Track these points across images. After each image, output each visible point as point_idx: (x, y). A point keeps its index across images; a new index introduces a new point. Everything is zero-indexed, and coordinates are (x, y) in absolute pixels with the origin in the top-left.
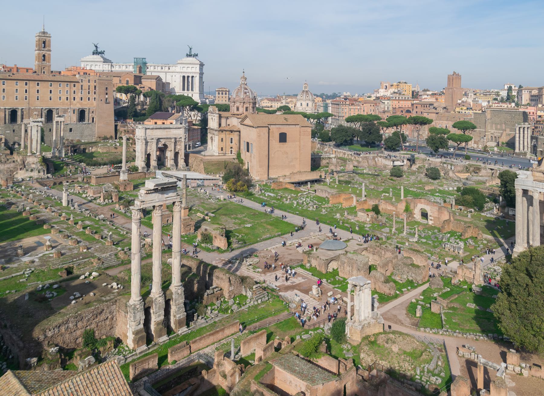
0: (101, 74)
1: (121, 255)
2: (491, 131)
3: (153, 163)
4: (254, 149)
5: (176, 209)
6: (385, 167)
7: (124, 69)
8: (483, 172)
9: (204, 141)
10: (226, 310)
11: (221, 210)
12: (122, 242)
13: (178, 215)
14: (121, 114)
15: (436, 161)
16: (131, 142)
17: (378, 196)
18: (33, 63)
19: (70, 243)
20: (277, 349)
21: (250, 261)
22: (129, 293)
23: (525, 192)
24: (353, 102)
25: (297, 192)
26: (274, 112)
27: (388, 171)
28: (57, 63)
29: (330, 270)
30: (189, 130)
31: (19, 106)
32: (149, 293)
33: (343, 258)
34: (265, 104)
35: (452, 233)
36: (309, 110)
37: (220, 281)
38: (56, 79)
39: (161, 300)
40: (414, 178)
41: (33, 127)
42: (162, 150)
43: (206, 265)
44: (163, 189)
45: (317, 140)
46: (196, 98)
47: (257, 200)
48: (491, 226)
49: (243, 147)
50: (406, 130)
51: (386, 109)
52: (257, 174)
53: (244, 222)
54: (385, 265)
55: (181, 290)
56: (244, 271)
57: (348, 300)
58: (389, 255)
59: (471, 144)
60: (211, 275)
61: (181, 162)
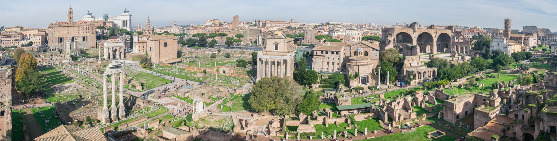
0: (90, 22)
1: (99, 92)
2: (249, 37)
3: (111, 57)
4: (153, 50)
5: (121, 75)
6: (208, 54)
7: (99, 19)
8: (246, 53)
9: (132, 47)
10: (142, 113)
11: (139, 75)
12: (100, 87)
13: (122, 77)
14: (98, 38)
15: (229, 51)
16: (102, 48)
17: (206, 66)
18: (67, 20)
19: (80, 86)
20: (164, 125)
21: (151, 95)
22: (103, 106)
23: (260, 59)
24: (195, 28)
25: (171, 67)
26: (162, 34)
27: (210, 56)
28: (75, 20)
29: (186, 96)
30: (126, 43)
31: (63, 36)
32: (110, 106)
33: (191, 92)
34: (158, 31)
35: (235, 77)
36: (177, 33)
37: (139, 102)
38: (75, 25)
39: (116, 109)
40: (220, 58)
41: (67, 43)
42: (115, 51)
43: (133, 97)
44: (116, 67)
45: (180, 45)
46: (128, 29)
47: (154, 71)
48: (249, 73)
49: (148, 49)
50: (217, 39)
51: (209, 31)
52: (154, 60)
53: (149, 80)
54: (209, 92)
55: (123, 105)
56: (150, 98)
57: (193, 107)
58: (210, 88)
59: (242, 43)
60: (135, 100)
61: (122, 56)
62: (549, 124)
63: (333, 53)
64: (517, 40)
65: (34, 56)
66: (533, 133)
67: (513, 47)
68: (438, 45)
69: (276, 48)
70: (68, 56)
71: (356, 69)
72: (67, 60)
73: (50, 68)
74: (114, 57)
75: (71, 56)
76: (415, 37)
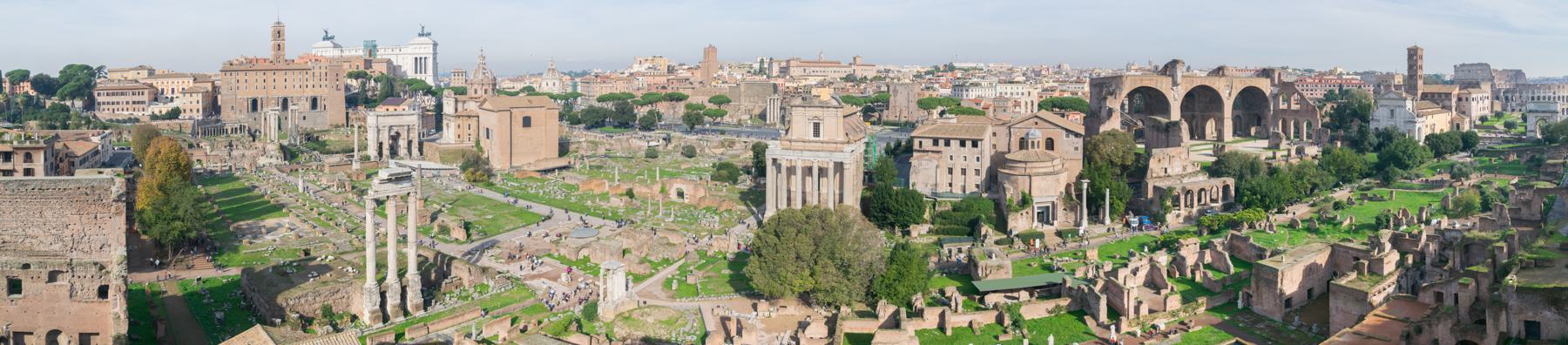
0: (331, 60)
1: (356, 242)
2: (745, 104)
3: (386, 152)
4: (494, 135)
5: (411, 199)
6: (640, 148)
7: (353, 53)
8: (738, 146)
9: (439, 128)
10: (466, 298)
11: (457, 202)
12: (356, 230)
13: (414, 205)
14: (352, 101)
15: (692, 139)
16: (363, 129)
17: (632, 180)
18: (269, 54)
19: (306, 227)
20: (523, 331)
21: (491, 252)
22: (365, 278)
23: (775, 160)
24: (605, 79)
25: (543, 181)
26: (516, 94)
27: (643, 153)
28: (290, 53)
29: (581, 257)
30: (423, 117)
31: (259, 95)
33: (595, 245)
34: (506, 85)
35: (708, 209)
36: (556, 91)
37: (459, 271)
38: (290, 67)
39: (398, 287)
40: (670, 157)
41: (271, 113)
43: (444, 256)
44: (397, 179)
45: (565, 123)
47: (498, 190)
48: (745, 197)
50: (662, 107)
51: (639, 87)
52: (498, 163)
54: (640, 247)
55: (418, 278)
56: (485, 261)
57: (600, 284)
58: (644, 237)
59: (727, 119)
60: (449, 265)
61: (415, 151)
62: (1522, 317)
63: (963, 144)
64: (1439, 100)
65: (185, 145)
66: (1482, 339)
67: (1430, 120)
68: (1236, 119)
69: (817, 133)
70: (273, 148)
71: (1023, 185)
72: (271, 158)
73: (227, 177)
74: (394, 152)
75: (282, 148)
76: (1175, 98)
